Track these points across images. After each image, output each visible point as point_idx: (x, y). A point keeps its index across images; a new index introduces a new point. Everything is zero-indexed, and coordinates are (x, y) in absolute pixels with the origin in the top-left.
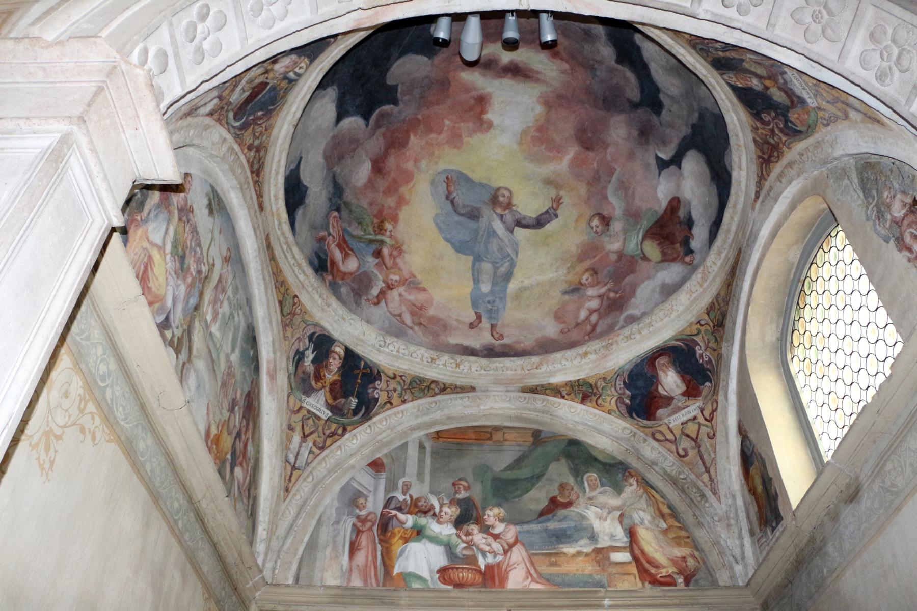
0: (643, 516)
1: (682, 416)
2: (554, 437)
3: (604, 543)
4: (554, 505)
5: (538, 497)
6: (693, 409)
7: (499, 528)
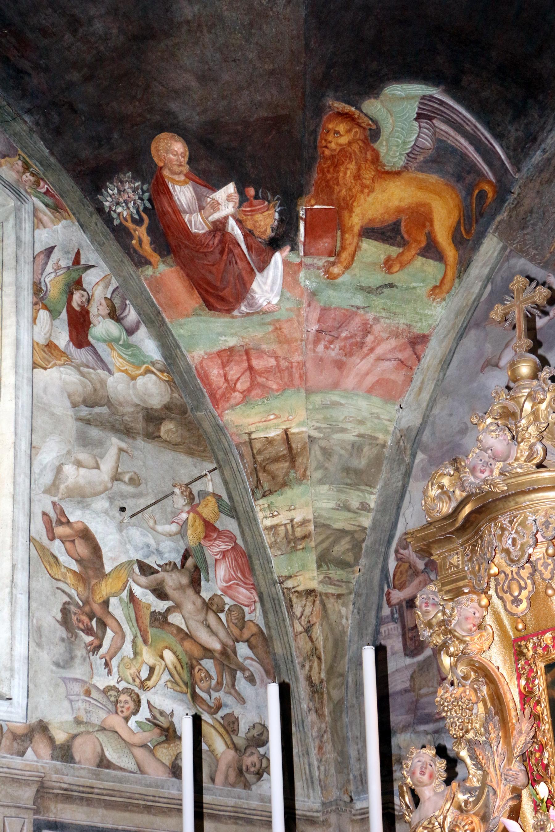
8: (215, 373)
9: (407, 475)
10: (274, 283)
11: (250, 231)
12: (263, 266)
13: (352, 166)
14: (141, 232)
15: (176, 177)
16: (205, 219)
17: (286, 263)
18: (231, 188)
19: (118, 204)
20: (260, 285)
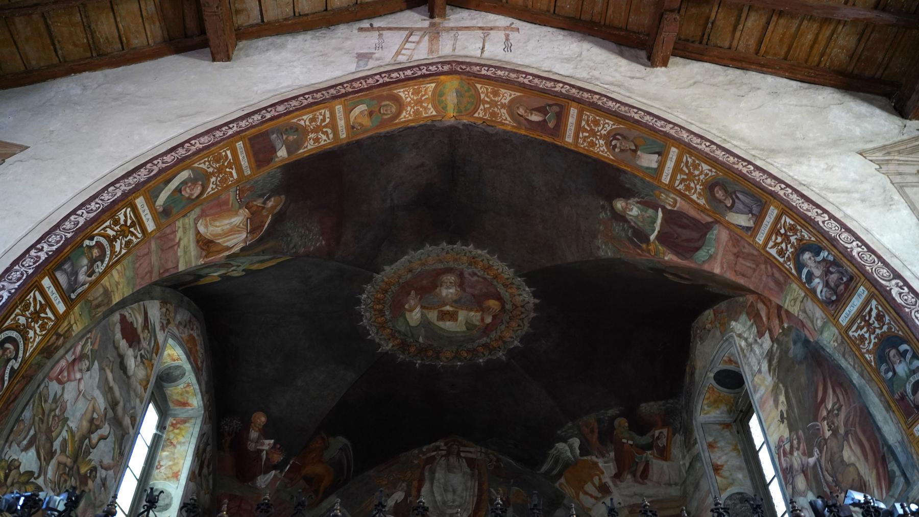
10: (267, 480)
11: (269, 459)
12: (267, 472)
13: (314, 455)
15: (255, 428)
16: (256, 446)
17: (275, 476)
18: (272, 441)
19: (227, 425)
20: (261, 479)
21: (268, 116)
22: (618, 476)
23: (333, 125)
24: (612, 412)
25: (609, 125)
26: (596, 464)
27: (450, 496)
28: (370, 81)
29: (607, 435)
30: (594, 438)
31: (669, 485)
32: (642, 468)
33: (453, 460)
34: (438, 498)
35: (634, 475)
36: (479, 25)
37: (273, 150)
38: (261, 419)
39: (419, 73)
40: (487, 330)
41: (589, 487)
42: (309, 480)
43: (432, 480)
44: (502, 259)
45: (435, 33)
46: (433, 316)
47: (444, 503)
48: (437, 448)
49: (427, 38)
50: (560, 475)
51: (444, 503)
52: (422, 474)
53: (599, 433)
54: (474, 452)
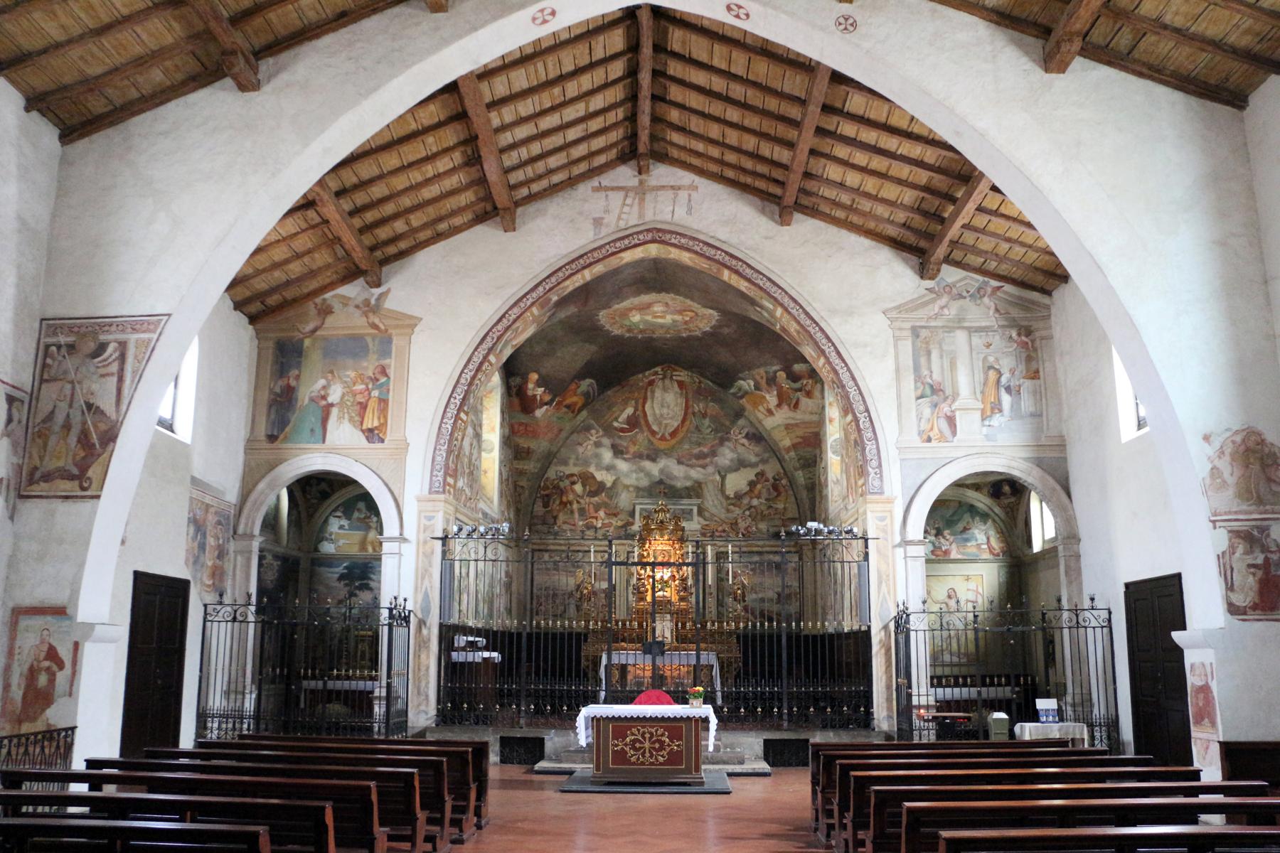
0: (992, 533)
1: (1009, 501)
2: (966, 504)
3: (980, 542)
4: (965, 530)
5: (960, 526)
6: (1013, 499)
7: (948, 537)
8: (516, 427)
9: (550, 463)
12: (541, 407)
14: (515, 390)
21: (547, 288)
22: (779, 406)
23: (583, 277)
24: (775, 368)
25: (746, 284)
26: (764, 397)
27: (665, 411)
28: (604, 251)
29: (772, 381)
30: (763, 382)
31: (812, 413)
32: (794, 402)
33: (667, 382)
34: (657, 412)
35: (789, 405)
36: (672, 184)
37: (551, 299)
38: (534, 376)
39: (633, 243)
40: (686, 323)
41: (761, 408)
42: (568, 407)
43: (653, 398)
44: (692, 299)
45: (641, 191)
46: (649, 318)
47: (662, 415)
48: (656, 373)
49: (637, 201)
50: (742, 397)
51: (662, 415)
52: (646, 393)
53: (767, 379)
54: (683, 375)
